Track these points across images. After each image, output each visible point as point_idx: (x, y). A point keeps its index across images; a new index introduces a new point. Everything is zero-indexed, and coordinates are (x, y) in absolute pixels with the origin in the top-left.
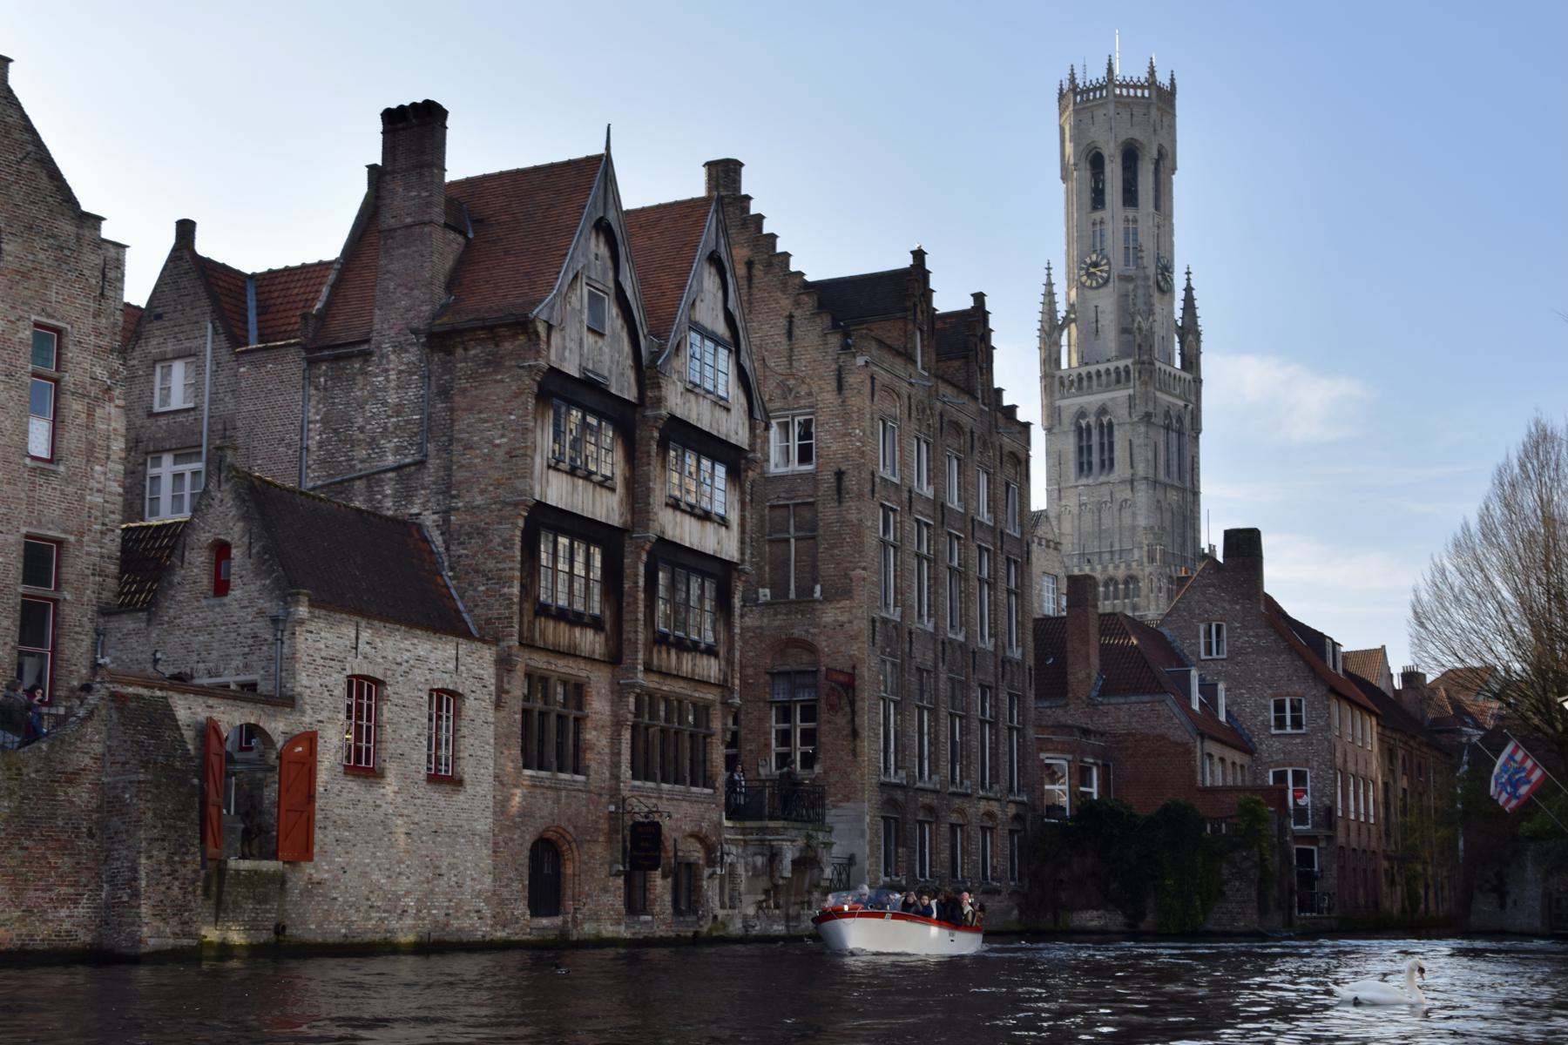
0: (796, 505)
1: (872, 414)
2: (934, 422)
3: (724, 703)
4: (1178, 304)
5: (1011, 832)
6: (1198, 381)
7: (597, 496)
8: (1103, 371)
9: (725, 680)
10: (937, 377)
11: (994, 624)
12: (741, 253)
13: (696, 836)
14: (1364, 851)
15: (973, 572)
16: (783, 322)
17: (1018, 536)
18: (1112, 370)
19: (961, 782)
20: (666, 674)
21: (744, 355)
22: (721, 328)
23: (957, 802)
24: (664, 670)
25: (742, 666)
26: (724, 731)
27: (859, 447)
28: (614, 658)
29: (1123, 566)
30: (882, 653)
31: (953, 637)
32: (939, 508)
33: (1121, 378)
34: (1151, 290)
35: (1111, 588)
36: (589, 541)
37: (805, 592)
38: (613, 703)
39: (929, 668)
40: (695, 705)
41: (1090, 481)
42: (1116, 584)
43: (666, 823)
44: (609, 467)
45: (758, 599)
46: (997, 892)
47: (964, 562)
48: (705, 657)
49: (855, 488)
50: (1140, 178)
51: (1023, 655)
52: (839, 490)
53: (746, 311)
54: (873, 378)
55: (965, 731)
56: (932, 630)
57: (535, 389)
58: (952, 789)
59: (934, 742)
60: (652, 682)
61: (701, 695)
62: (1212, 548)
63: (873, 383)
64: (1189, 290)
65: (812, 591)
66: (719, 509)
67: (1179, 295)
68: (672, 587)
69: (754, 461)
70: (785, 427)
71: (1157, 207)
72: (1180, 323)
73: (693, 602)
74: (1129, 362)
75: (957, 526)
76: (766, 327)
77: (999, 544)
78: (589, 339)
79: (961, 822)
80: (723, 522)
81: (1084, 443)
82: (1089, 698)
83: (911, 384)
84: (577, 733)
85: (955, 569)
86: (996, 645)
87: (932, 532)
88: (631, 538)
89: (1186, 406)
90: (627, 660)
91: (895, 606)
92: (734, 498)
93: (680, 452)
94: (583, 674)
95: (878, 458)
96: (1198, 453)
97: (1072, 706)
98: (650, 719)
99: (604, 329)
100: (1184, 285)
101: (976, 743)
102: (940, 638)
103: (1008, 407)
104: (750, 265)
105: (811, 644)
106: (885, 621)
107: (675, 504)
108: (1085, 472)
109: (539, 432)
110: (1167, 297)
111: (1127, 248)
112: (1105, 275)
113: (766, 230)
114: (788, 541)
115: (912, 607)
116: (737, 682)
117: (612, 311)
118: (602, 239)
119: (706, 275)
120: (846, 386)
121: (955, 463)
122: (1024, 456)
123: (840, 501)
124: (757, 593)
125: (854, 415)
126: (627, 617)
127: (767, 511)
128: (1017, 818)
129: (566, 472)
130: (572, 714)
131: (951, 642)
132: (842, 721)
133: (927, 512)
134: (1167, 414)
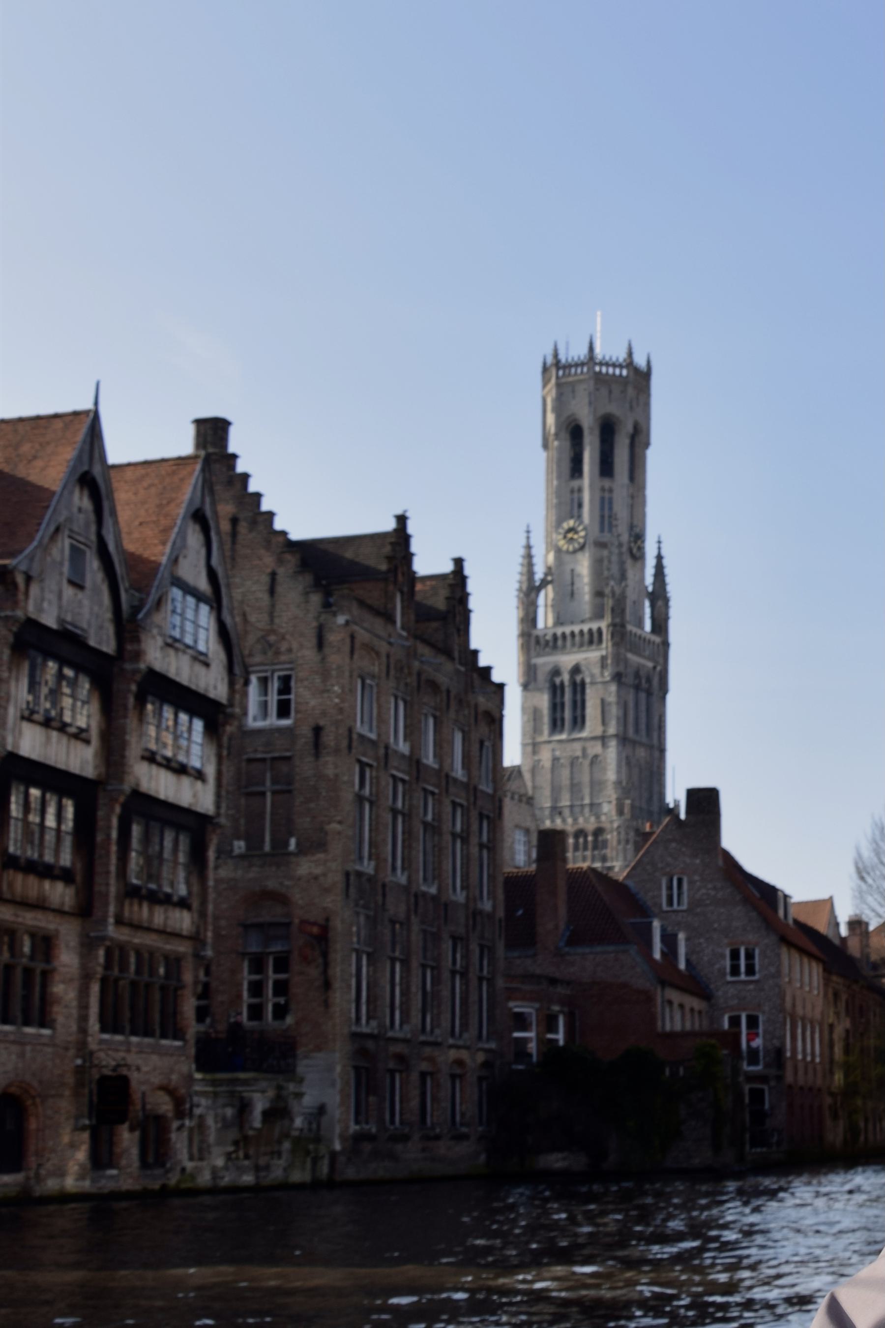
0: (274, 759)
1: (351, 672)
3: (197, 956)
5: (480, 1079)
9: (198, 932)
13: (165, 1088)
14: (811, 1089)
20: (137, 927)
23: (428, 1050)
25: (216, 918)
26: (196, 982)
27: (337, 704)
36: (61, 793)
37: (280, 844)
42: (586, 836)
43: (134, 1076)
45: (232, 851)
49: (332, 744)
53: (229, 566)
54: (352, 637)
55: (436, 981)
57: (11, 639)
59: (405, 993)
60: (121, 935)
62: (677, 806)
66: (195, 762)
68: (146, 839)
69: (232, 716)
70: (264, 682)
73: (167, 854)
76: (249, 583)
78: (69, 592)
80: (199, 775)
84: (45, 985)
86: (467, 898)
87: (407, 786)
91: (370, 858)
92: (211, 752)
93: (157, 705)
95: (355, 714)
101: (446, 993)
106: (359, 874)
107: (151, 758)
109: (13, 684)
114: (263, 794)
115: (386, 860)
116: (210, 934)
118: (86, 493)
124: (231, 845)
125: (334, 673)
130: (39, 966)
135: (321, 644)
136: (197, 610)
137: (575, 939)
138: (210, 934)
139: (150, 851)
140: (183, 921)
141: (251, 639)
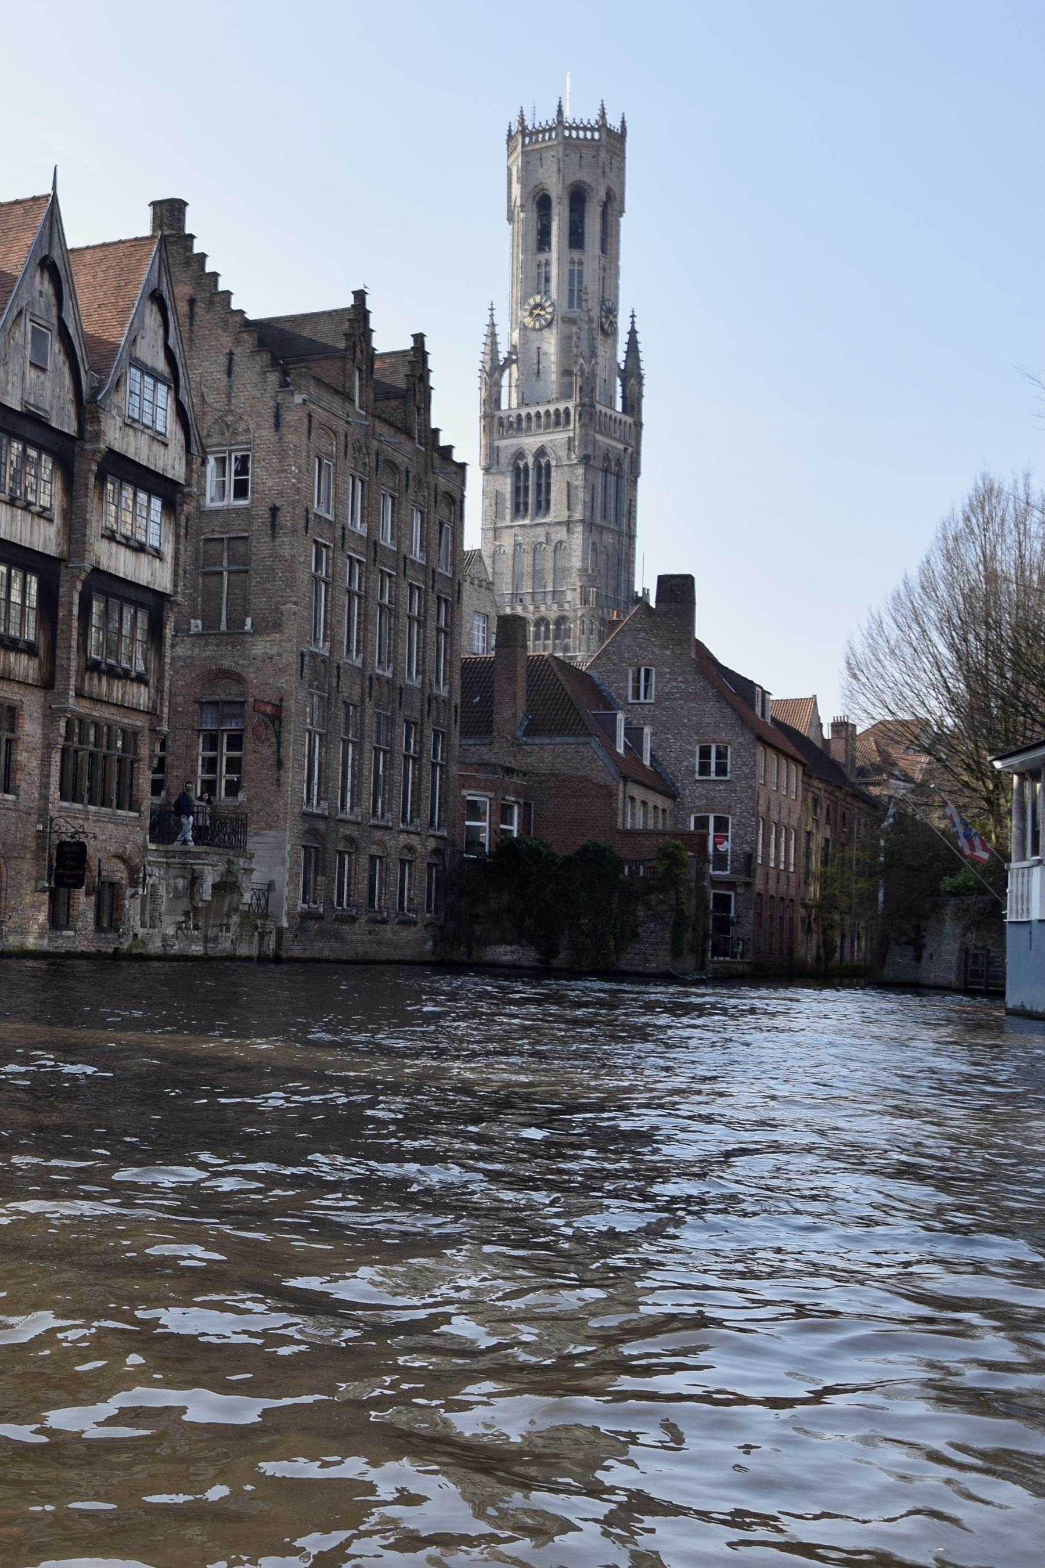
0: (230, 539)
1: (308, 452)
2: (371, 460)
4: (622, 348)
5: (430, 866)
6: (639, 425)
7: (35, 527)
8: (542, 413)
9: (155, 708)
10: (374, 416)
11: (422, 662)
12: (184, 290)
15: (403, 610)
16: (223, 360)
17: (450, 576)
18: (552, 412)
19: (383, 815)
20: (96, 700)
21: (182, 390)
22: (161, 365)
23: (378, 834)
24: (95, 696)
27: (294, 484)
28: (48, 683)
29: (555, 607)
30: (310, 687)
31: (381, 672)
32: (371, 545)
33: (560, 420)
34: (595, 333)
35: (542, 629)
37: (237, 623)
38: (44, 727)
39: (355, 702)
40: (123, 731)
41: (527, 522)
44: (48, 498)
46: (412, 923)
47: (395, 600)
48: (135, 684)
50: (587, 221)
51: (450, 692)
52: (273, 525)
54: (310, 416)
55: (389, 765)
56: (360, 666)
58: (372, 822)
59: (358, 775)
60: (83, 708)
61: (131, 722)
63: (310, 421)
64: (633, 333)
65: (244, 624)
66: (153, 541)
67: (623, 338)
68: (106, 616)
69: (190, 495)
70: (222, 462)
71: (603, 250)
72: (622, 367)
74: (571, 405)
75: (389, 564)
77: (430, 583)
79: (381, 854)
81: (522, 484)
82: (513, 737)
83: (348, 422)
85: (385, 606)
86: (423, 682)
87: (364, 568)
88: (67, 567)
89: (626, 449)
90: (59, 686)
91: (325, 641)
92: (169, 531)
93: (117, 485)
94: (17, 697)
95: (313, 494)
96: (635, 497)
97: (497, 745)
98: (80, 742)
99: (46, 364)
100: (629, 329)
102: (368, 673)
103: (444, 447)
104: (192, 302)
105: (239, 675)
106: (314, 655)
108: (522, 513)
110: (610, 341)
111: (571, 291)
112: (549, 317)
113: (208, 269)
114: (221, 573)
116: (166, 710)
117: (54, 347)
119: (147, 312)
120: (283, 423)
121: (390, 501)
122: (459, 496)
123: (273, 537)
124: (189, 624)
126: (60, 643)
127: (201, 544)
128: (436, 852)
129: (6, 503)
131: (379, 678)
132: (267, 751)
133: (360, 549)
134: (606, 457)
135: (277, 425)
136: (155, 390)
137: (528, 733)
138: (166, 710)
139: (111, 626)
140: (140, 696)
141: (209, 419)
